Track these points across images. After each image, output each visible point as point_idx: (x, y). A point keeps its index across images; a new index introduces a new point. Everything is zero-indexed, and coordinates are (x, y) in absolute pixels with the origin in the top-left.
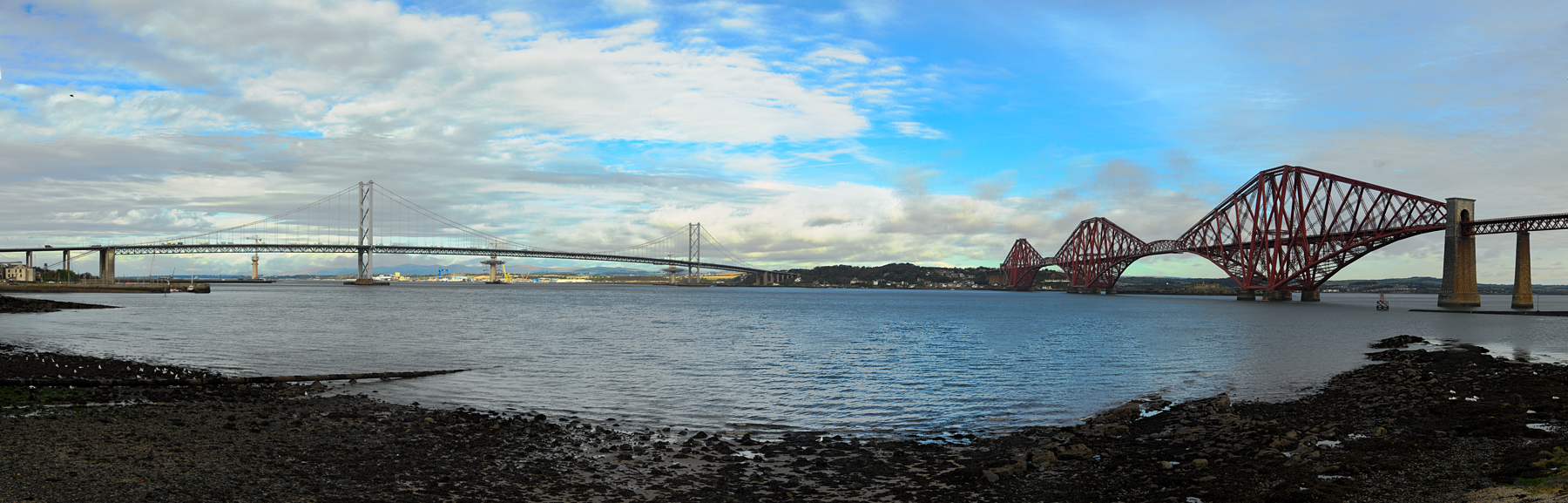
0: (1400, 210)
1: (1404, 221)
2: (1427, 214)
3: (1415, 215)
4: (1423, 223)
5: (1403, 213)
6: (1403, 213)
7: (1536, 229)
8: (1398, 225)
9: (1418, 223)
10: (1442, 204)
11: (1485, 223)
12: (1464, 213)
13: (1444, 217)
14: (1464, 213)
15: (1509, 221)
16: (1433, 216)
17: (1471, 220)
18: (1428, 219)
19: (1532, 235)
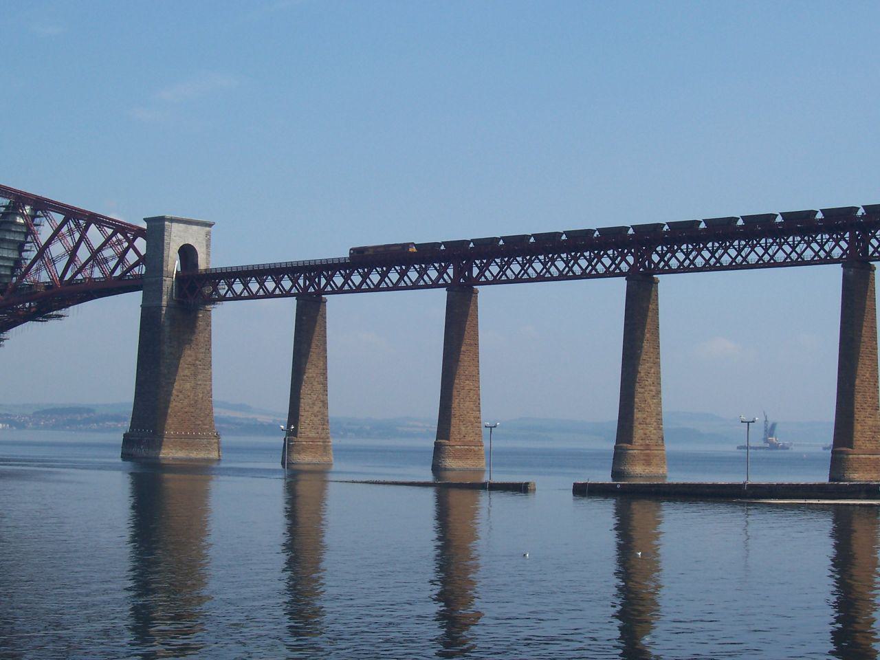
0: (49, 242)
1: (60, 267)
2: (108, 253)
3: (83, 254)
4: (97, 273)
5: (57, 249)
6: (57, 249)
7: (340, 291)
8: (44, 277)
9: (87, 273)
10: (139, 232)
11: (230, 275)
12: (187, 253)
13: (142, 260)
14: (187, 253)
15: (277, 272)
16: (122, 257)
17: (202, 265)
18: (112, 264)
19: (333, 304)
